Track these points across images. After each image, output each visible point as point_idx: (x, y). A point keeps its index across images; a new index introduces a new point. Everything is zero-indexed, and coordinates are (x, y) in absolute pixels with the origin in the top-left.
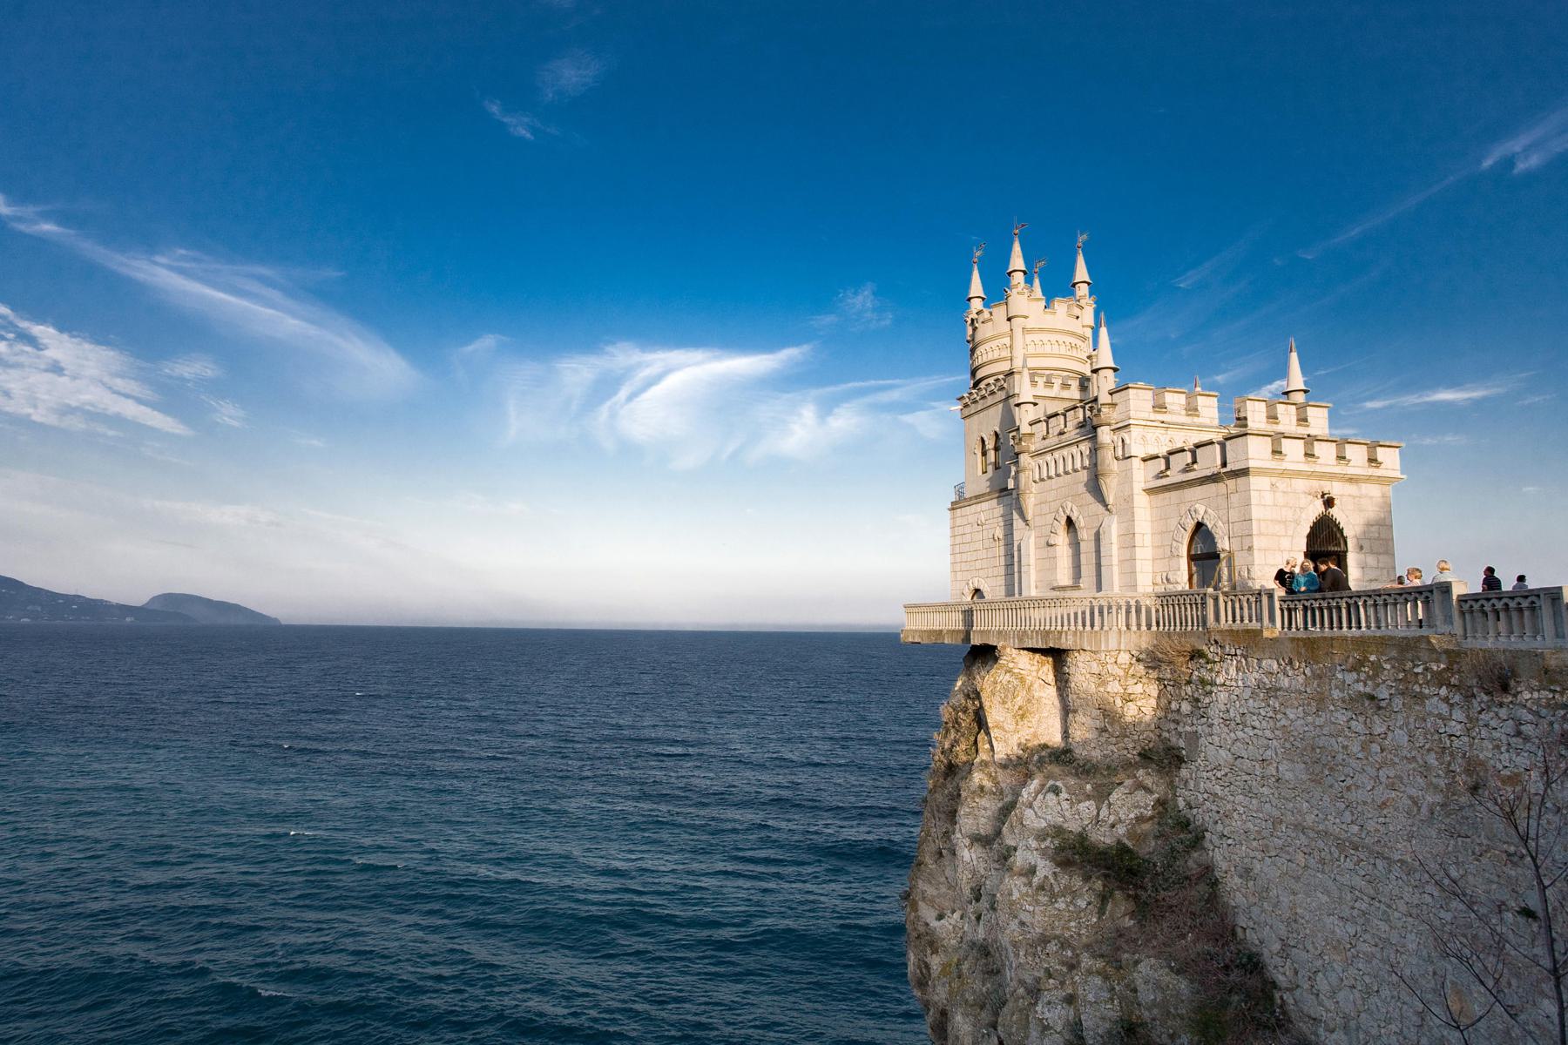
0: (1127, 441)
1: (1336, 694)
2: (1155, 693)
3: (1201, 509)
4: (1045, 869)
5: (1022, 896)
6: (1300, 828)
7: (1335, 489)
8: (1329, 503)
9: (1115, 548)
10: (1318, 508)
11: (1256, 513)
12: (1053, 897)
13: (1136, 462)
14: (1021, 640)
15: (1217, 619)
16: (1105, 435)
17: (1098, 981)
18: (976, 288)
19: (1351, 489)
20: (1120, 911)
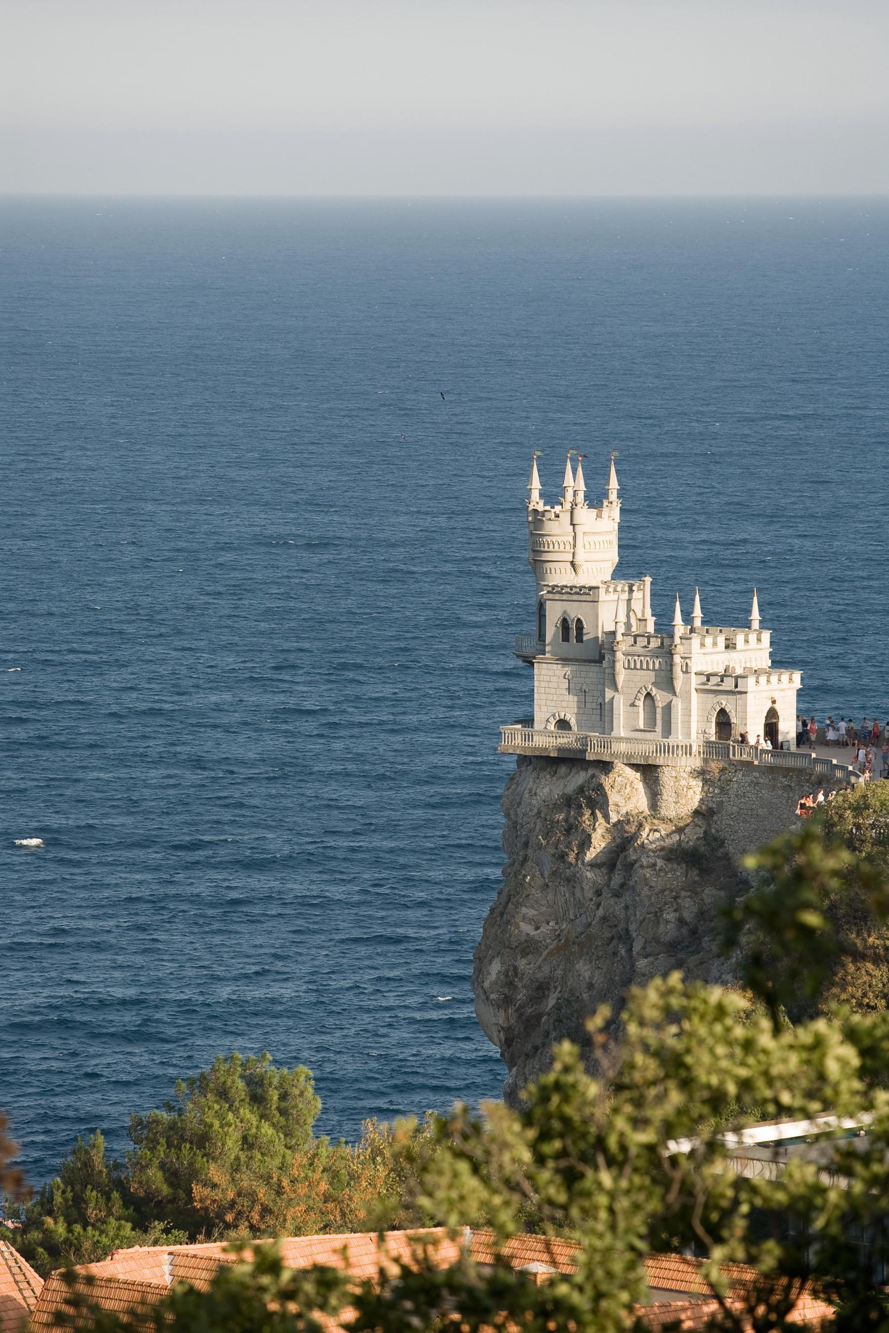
0: (689, 665)
1: (779, 785)
2: (701, 784)
3: (724, 703)
4: (660, 863)
5: (651, 875)
6: (765, 830)
7: (776, 695)
8: (774, 702)
9: (680, 714)
10: (769, 705)
11: (749, 709)
12: (666, 873)
13: (693, 675)
14: (628, 759)
15: (734, 755)
16: (677, 659)
17: (689, 900)
18: (536, 483)
19: (782, 694)
20: (694, 874)
